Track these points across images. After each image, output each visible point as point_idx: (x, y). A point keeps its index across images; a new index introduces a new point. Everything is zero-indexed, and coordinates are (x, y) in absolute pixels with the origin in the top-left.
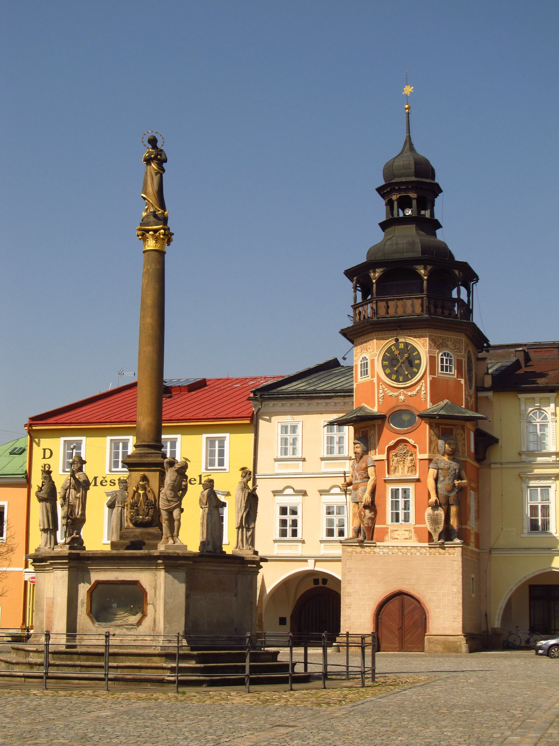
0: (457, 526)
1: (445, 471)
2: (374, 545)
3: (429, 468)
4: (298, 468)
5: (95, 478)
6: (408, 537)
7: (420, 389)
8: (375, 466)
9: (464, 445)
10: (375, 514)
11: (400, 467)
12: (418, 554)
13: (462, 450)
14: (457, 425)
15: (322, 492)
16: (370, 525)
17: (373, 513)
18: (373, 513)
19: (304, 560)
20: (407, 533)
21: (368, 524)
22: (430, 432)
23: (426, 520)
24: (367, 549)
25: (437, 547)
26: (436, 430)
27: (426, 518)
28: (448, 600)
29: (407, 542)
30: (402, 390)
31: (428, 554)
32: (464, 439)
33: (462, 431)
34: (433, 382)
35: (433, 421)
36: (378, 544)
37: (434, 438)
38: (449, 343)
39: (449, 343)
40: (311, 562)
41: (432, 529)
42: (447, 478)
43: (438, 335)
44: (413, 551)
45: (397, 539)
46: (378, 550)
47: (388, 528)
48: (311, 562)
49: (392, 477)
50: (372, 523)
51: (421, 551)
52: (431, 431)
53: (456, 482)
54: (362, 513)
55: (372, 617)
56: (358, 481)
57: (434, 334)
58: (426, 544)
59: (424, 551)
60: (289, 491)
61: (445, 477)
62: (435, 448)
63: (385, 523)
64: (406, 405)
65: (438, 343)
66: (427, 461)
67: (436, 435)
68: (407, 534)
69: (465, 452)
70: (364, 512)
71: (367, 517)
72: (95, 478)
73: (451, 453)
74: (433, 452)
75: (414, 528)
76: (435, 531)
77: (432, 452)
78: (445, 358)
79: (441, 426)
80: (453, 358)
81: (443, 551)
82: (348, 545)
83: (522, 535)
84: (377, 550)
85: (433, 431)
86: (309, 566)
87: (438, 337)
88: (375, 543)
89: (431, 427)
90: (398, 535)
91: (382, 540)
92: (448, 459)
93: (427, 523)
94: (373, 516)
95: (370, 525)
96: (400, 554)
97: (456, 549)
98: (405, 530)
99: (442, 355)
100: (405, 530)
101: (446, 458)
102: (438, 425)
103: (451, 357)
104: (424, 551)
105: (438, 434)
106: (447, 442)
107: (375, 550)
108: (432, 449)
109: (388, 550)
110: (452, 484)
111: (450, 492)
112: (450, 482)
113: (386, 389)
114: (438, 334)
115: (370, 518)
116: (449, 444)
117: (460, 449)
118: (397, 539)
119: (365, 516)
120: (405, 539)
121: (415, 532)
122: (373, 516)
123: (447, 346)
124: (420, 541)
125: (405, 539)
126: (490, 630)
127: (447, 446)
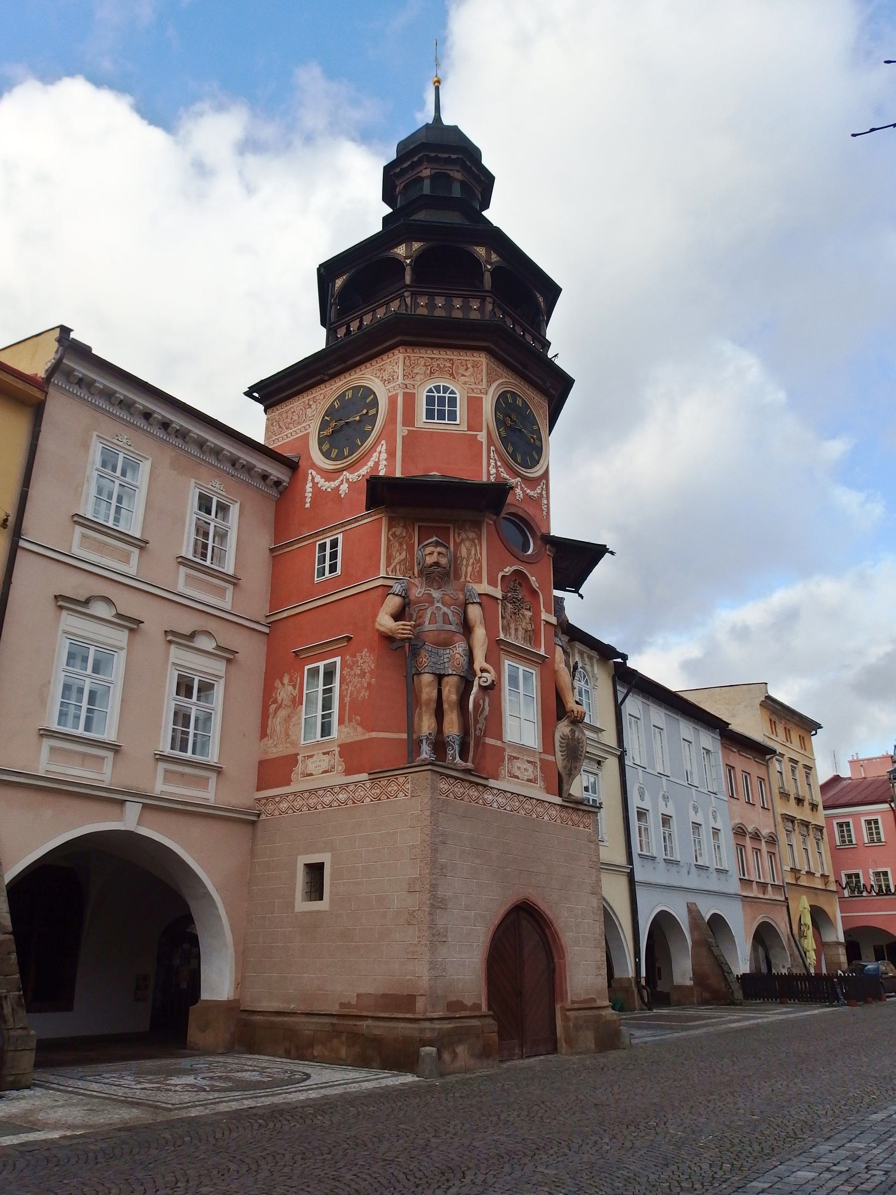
4: (127, 562)
6: (532, 777)
7: (541, 494)
15: (174, 637)
19: (115, 800)
20: (530, 767)
23: (557, 749)
27: (557, 744)
29: (531, 787)
31: (559, 821)
36: (492, 783)
40: (133, 810)
41: (565, 768)
45: (517, 777)
46: (490, 797)
48: (133, 810)
54: (481, 702)
56: (452, 628)
58: (557, 800)
59: (554, 813)
60: (100, 609)
63: (500, 737)
68: (530, 774)
75: (541, 760)
82: (441, 774)
84: (489, 797)
86: (129, 820)
90: (519, 768)
91: (496, 778)
93: (559, 754)
96: (522, 812)
98: (529, 762)
100: (529, 762)
113: (499, 464)
118: (517, 777)
120: (528, 780)
125: (528, 780)
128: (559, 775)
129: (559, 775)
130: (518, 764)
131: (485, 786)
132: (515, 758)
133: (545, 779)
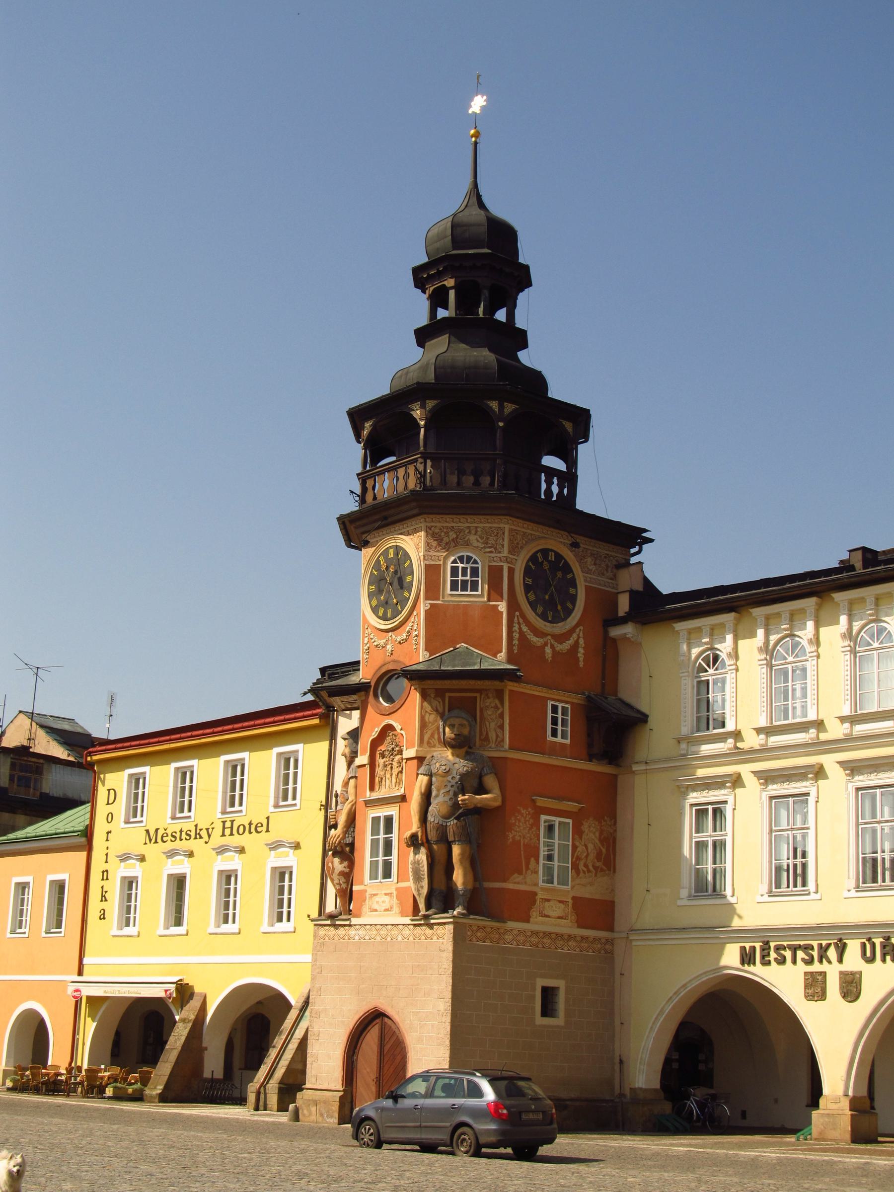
0: (464, 884)
1: (441, 779)
2: (348, 923)
3: (418, 774)
5: (157, 830)
6: (388, 906)
8: (356, 777)
9: (502, 727)
10: (351, 865)
11: (388, 776)
12: (400, 938)
13: (497, 736)
14: (486, 690)
16: (344, 886)
17: (346, 863)
18: (346, 863)
20: (387, 898)
21: (340, 885)
22: (422, 707)
24: (341, 931)
25: (420, 925)
26: (435, 703)
28: (433, 1025)
30: (390, 634)
32: (502, 716)
33: (497, 702)
34: (432, 616)
35: (429, 684)
36: (354, 921)
37: (431, 717)
38: (473, 538)
39: (473, 538)
42: (442, 791)
43: (447, 524)
44: (395, 932)
45: (376, 910)
47: (366, 891)
49: (375, 795)
50: (347, 882)
51: (404, 932)
52: (425, 704)
53: (460, 798)
55: (342, 1057)
57: (438, 524)
61: (438, 790)
62: (432, 736)
64: (394, 661)
65: (446, 539)
66: (415, 761)
67: (437, 710)
69: (503, 740)
70: (332, 863)
71: (337, 872)
72: (157, 830)
73: (453, 742)
74: (428, 743)
75: (397, 889)
76: (419, 895)
77: (425, 744)
78: (461, 565)
79: (447, 695)
80: (480, 566)
81: (431, 932)
82: (320, 925)
83: (680, 903)
84: (352, 932)
85: (430, 703)
87: (447, 528)
88: (349, 919)
89: (424, 696)
90: (377, 902)
92: (453, 755)
94: (347, 870)
95: (344, 886)
97: (446, 926)
98: (386, 894)
99: (454, 562)
100: (386, 894)
101: (448, 754)
102: (440, 693)
103: (475, 562)
104: (406, 931)
105: (441, 710)
106: (448, 723)
107: (350, 932)
108: (426, 738)
109: (364, 933)
110: (450, 803)
111: (447, 817)
112: (447, 798)
114: (442, 522)
115: (342, 873)
116: (452, 727)
117: (492, 735)
118: (376, 910)
119: (333, 869)
121: (398, 898)
122: (347, 870)
123: (467, 544)
124: (403, 914)
126: (627, 1092)
127: (447, 729)
128: (414, 896)
129: (414, 896)
130: (376, 898)
131: (350, 925)
132: (375, 895)
133: (401, 904)
